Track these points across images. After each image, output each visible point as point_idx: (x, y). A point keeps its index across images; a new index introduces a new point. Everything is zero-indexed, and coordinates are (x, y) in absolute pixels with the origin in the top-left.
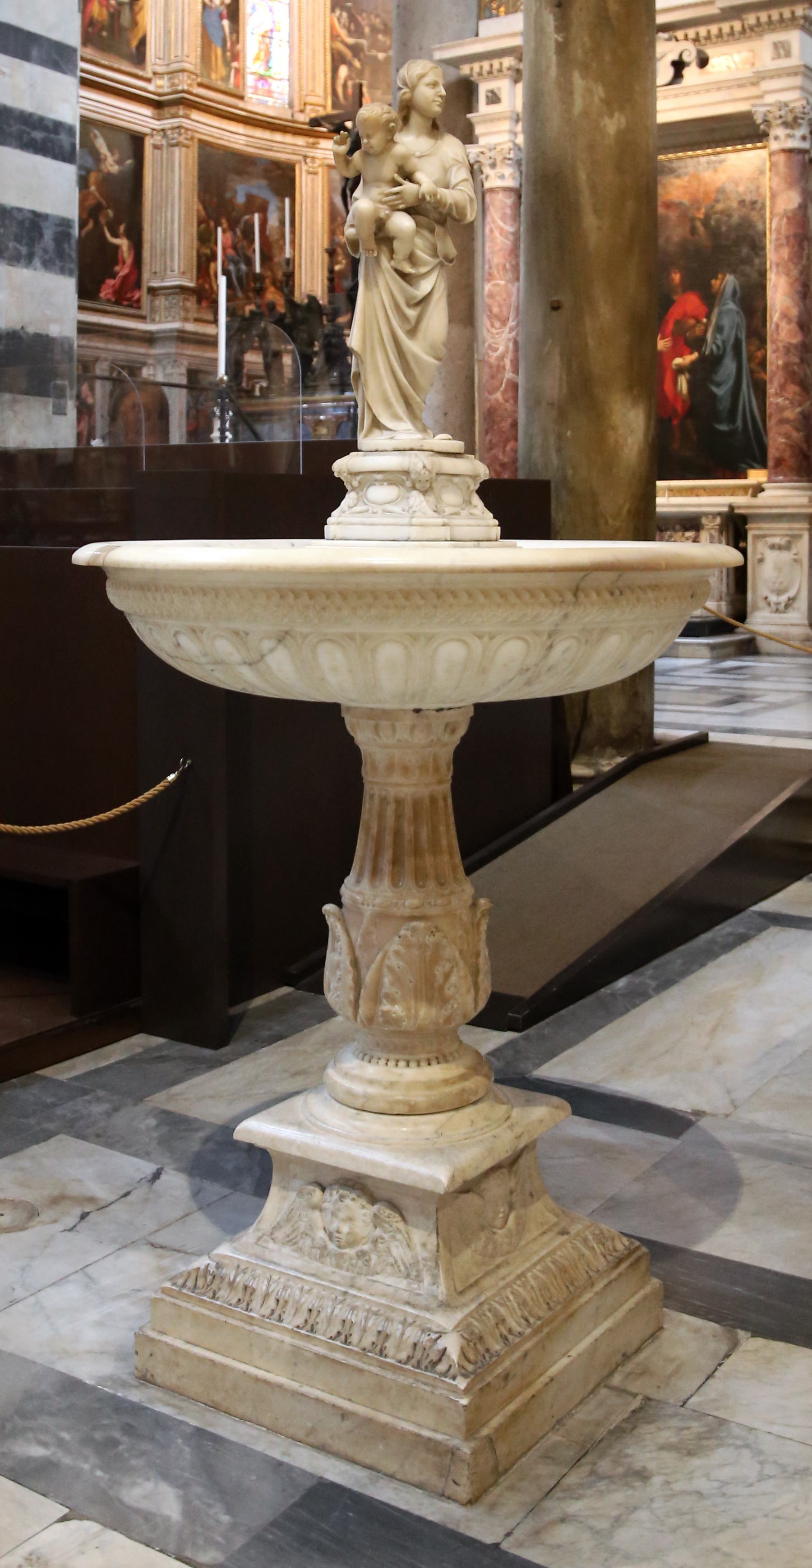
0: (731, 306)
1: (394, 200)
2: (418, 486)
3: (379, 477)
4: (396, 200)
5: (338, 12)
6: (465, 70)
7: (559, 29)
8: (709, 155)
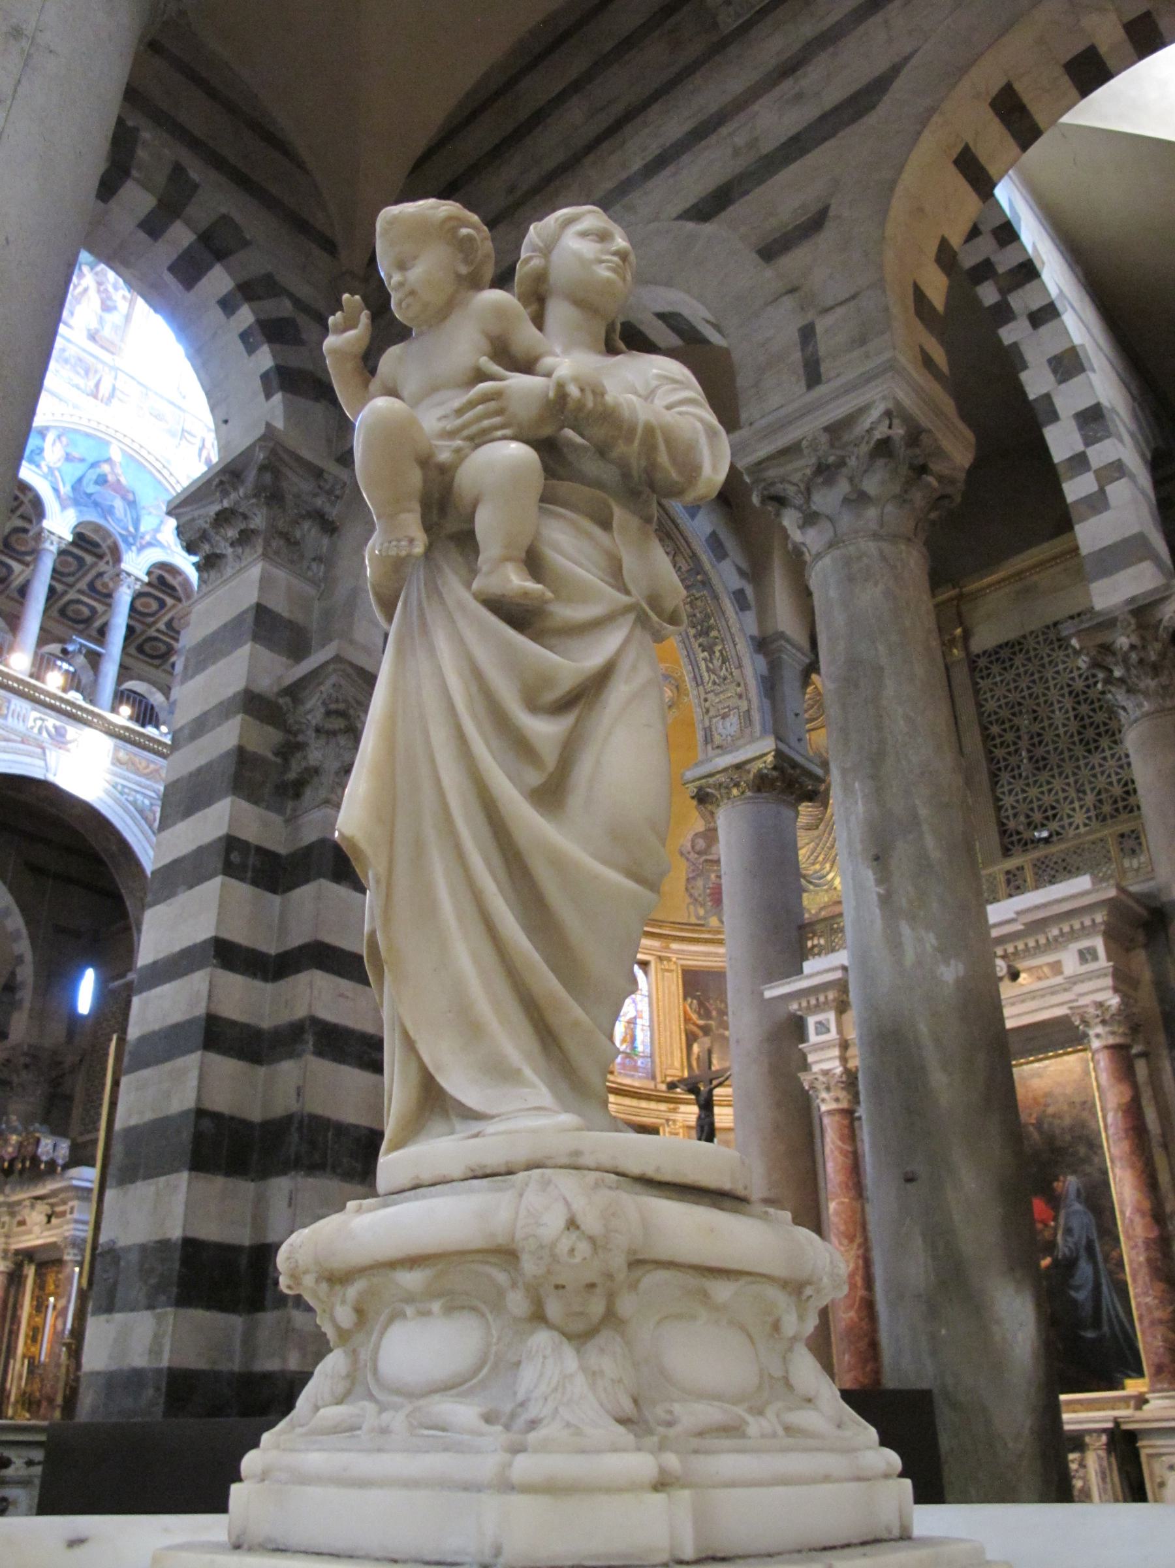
0: (1078, 1206)
1: (479, 419)
2: (553, 1309)
3: (411, 1279)
4: (488, 415)
5: (689, 1000)
6: (794, 1006)
7: (879, 882)
8: (1032, 1062)
